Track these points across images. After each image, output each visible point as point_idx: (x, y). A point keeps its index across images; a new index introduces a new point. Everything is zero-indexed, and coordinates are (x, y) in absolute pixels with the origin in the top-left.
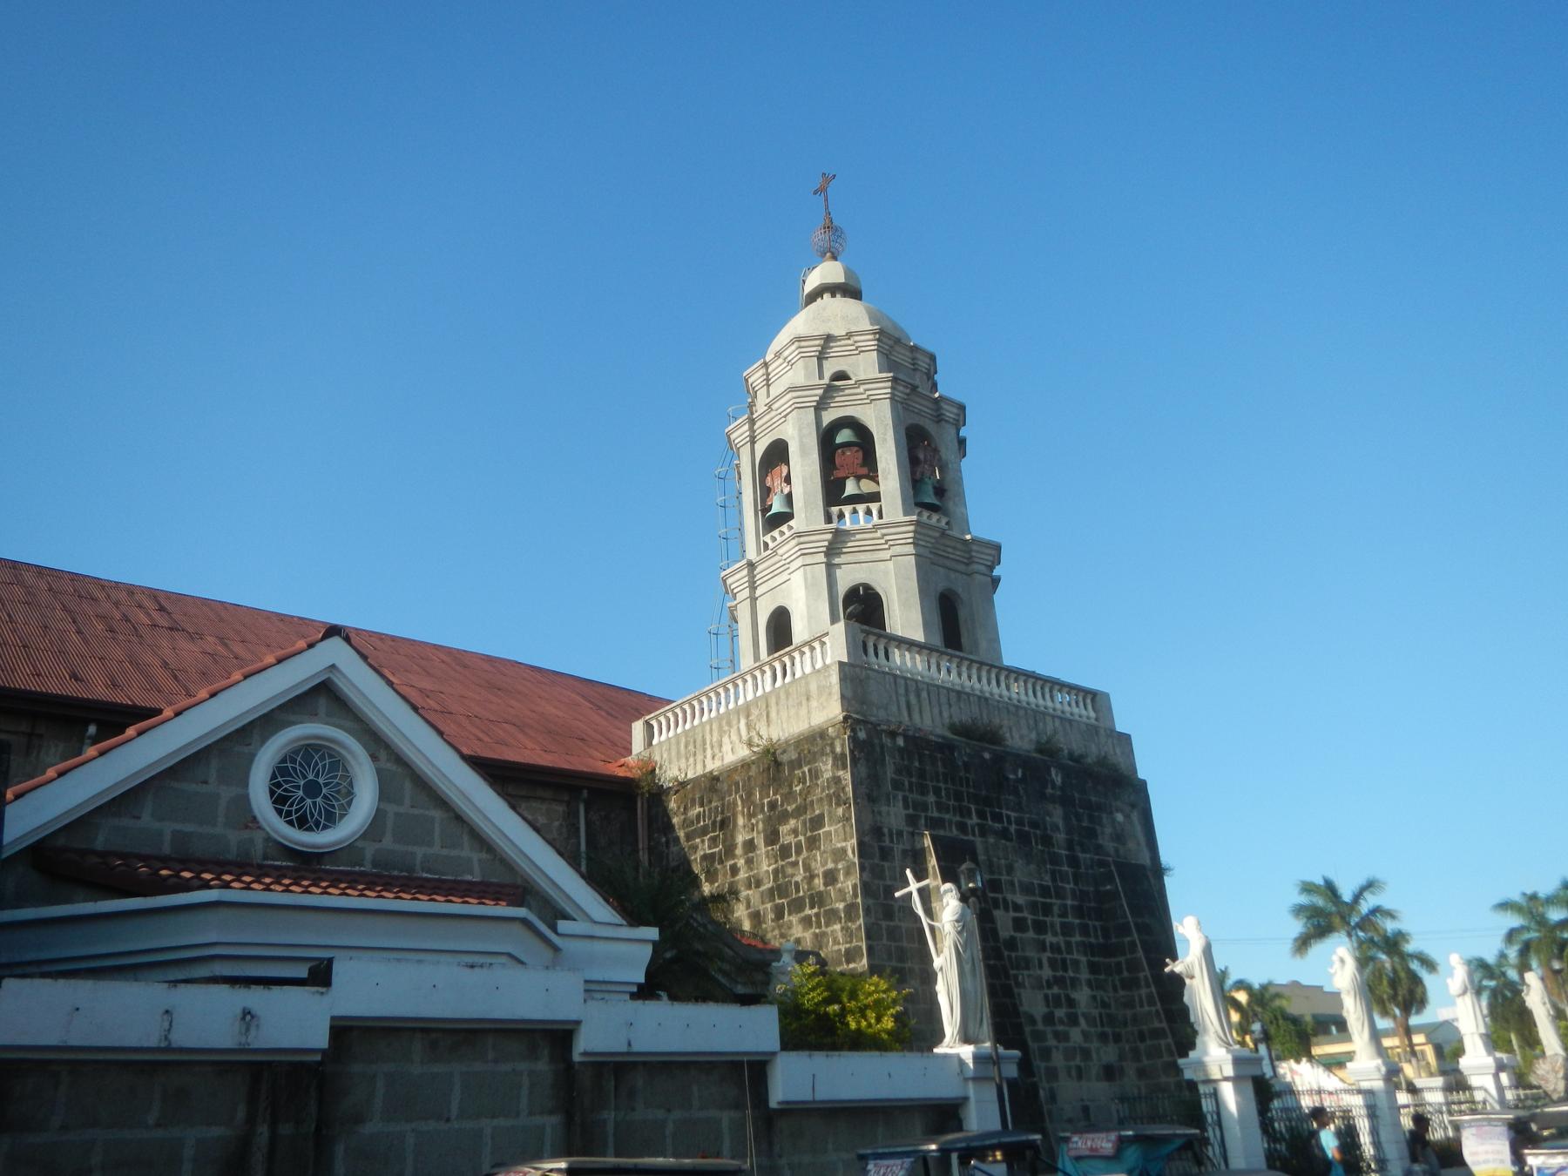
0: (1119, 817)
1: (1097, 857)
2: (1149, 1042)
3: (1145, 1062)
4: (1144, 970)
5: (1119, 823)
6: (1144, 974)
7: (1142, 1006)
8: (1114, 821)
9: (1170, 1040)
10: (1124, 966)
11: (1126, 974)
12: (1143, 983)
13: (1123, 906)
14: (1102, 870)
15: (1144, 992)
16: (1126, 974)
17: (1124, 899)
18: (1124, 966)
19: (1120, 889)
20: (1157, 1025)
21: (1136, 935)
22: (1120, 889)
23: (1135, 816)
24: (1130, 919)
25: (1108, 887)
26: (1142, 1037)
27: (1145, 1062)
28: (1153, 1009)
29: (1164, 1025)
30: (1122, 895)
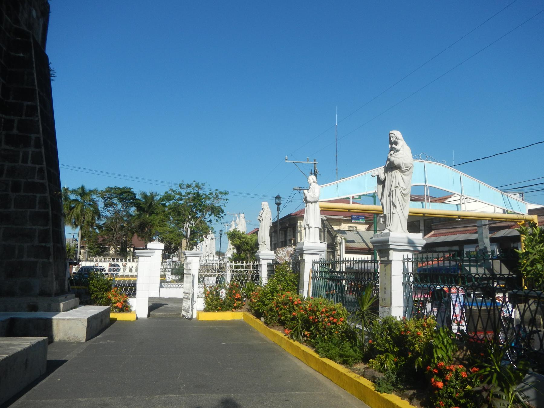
0: (34, 13)
1: (15, 26)
2: (22, 193)
3: (12, 209)
4: (38, 132)
5: (33, 17)
6: (37, 136)
7: (25, 161)
8: (30, 13)
9: (47, 195)
10: (15, 125)
11: (15, 131)
12: (32, 143)
13: (33, 74)
14: (19, 39)
15: (31, 150)
16: (15, 131)
17: (35, 69)
18: (15, 125)
19: (34, 60)
20: (37, 180)
21: (38, 104)
22: (34, 60)
23: (41, 22)
24: (37, 88)
25: (21, 55)
26: (16, 188)
27: (12, 209)
28: (37, 166)
29: (45, 181)
30: (34, 65)
